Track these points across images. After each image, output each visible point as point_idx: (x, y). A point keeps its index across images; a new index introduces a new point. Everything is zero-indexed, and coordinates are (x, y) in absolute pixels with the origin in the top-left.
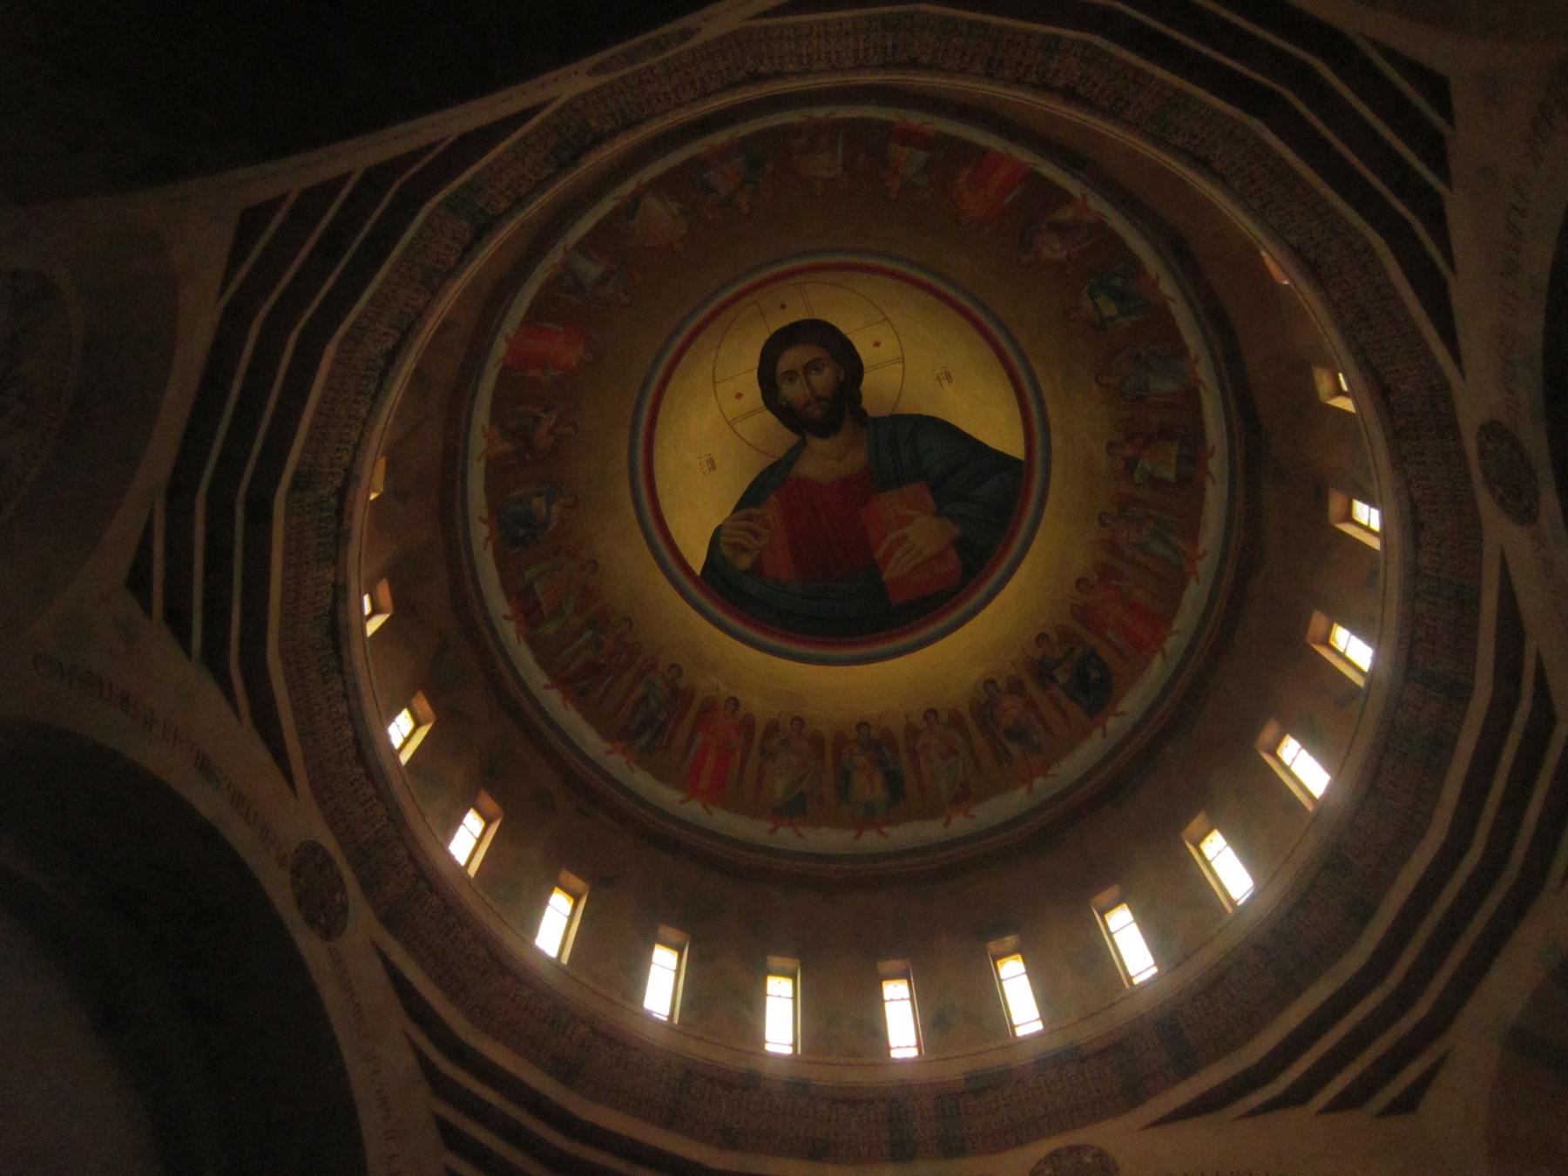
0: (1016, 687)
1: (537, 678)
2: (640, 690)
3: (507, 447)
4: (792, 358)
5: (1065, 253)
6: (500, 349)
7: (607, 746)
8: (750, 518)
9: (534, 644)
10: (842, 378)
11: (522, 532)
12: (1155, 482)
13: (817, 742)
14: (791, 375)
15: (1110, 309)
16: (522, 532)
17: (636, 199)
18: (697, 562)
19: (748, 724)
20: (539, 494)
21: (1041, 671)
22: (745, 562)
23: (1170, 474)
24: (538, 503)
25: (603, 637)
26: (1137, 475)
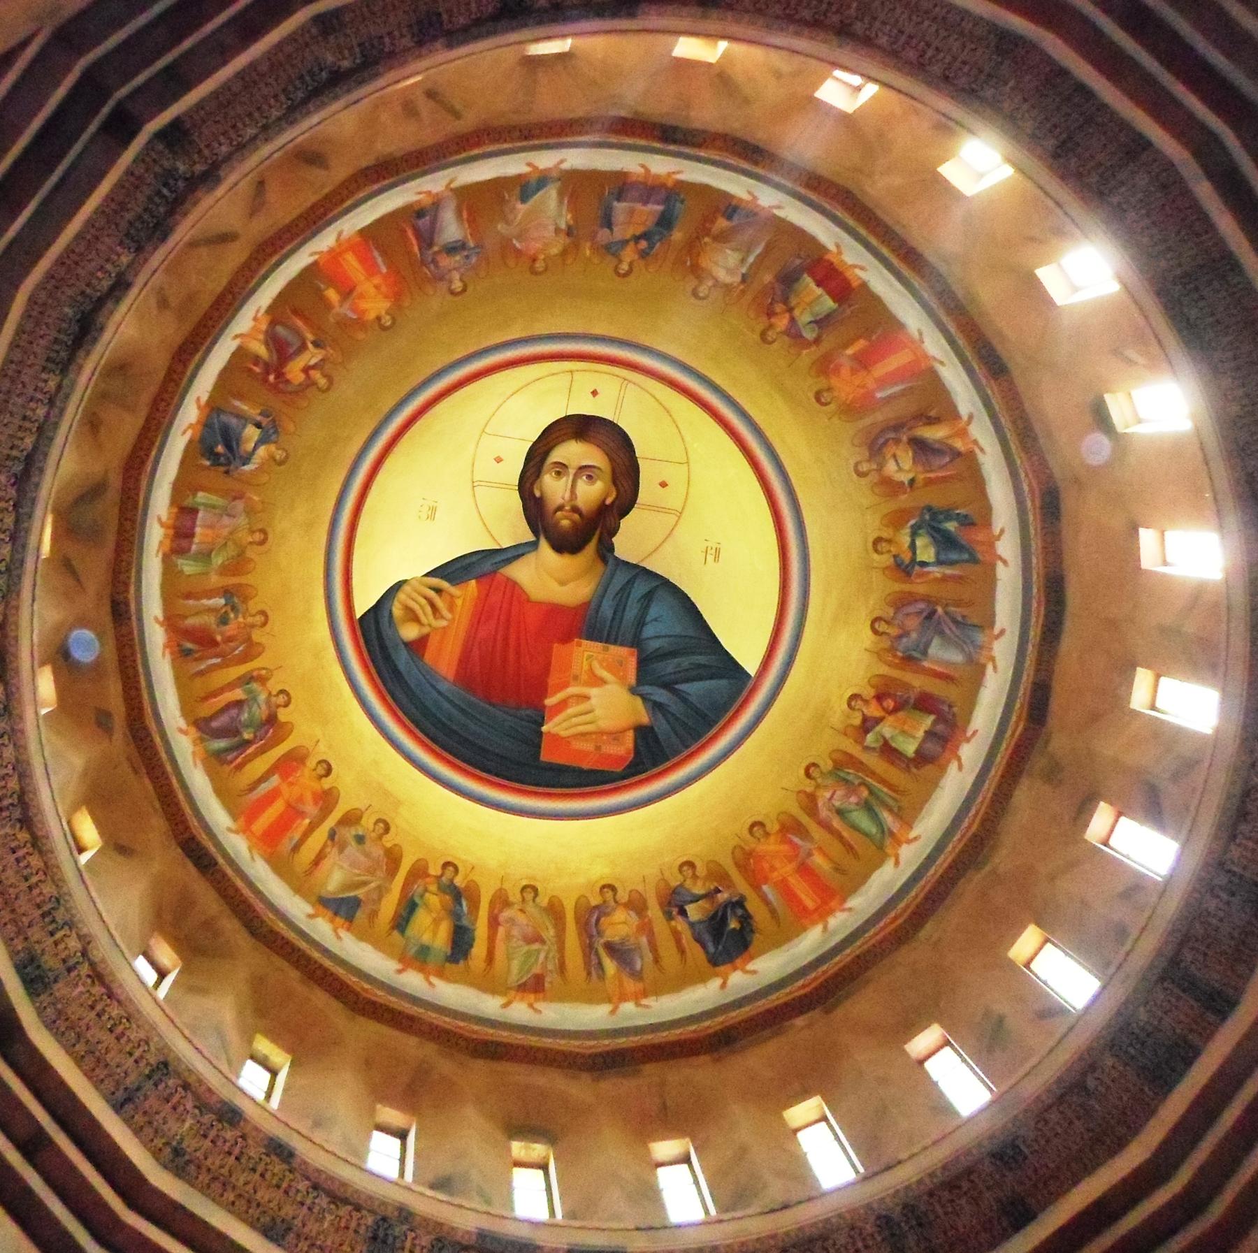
0: (637, 905)
1: (153, 606)
2: (238, 694)
3: (261, 349)
4: (572, 452)
5: (911, 476)
6: (325, 241)
7: (182, 723)
8: (438, 591)
9: (170, 572)
10: (608, 501)
11: (220, 449)
12: (888, 751)
13: (393, 859)
14: (561, 469)
15: (926, 551)
16: (220, 449)
17: (543, 180)
18: (362, 606)
19: (327, 800)
20: (258, 425)
21: (675, 902)
22: (410, 632)
23: (910, 748)
24: (251, 433)
25: (232, 615)
26: (870, 738)
